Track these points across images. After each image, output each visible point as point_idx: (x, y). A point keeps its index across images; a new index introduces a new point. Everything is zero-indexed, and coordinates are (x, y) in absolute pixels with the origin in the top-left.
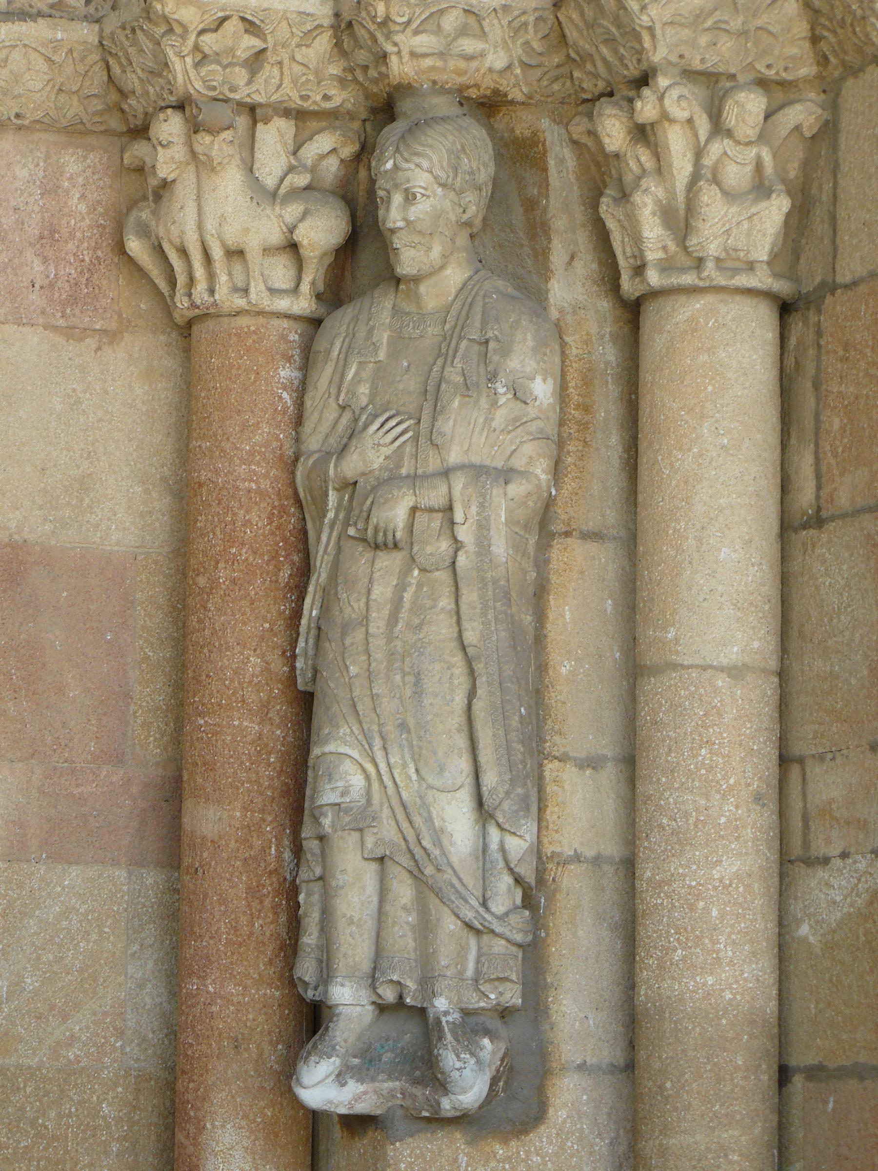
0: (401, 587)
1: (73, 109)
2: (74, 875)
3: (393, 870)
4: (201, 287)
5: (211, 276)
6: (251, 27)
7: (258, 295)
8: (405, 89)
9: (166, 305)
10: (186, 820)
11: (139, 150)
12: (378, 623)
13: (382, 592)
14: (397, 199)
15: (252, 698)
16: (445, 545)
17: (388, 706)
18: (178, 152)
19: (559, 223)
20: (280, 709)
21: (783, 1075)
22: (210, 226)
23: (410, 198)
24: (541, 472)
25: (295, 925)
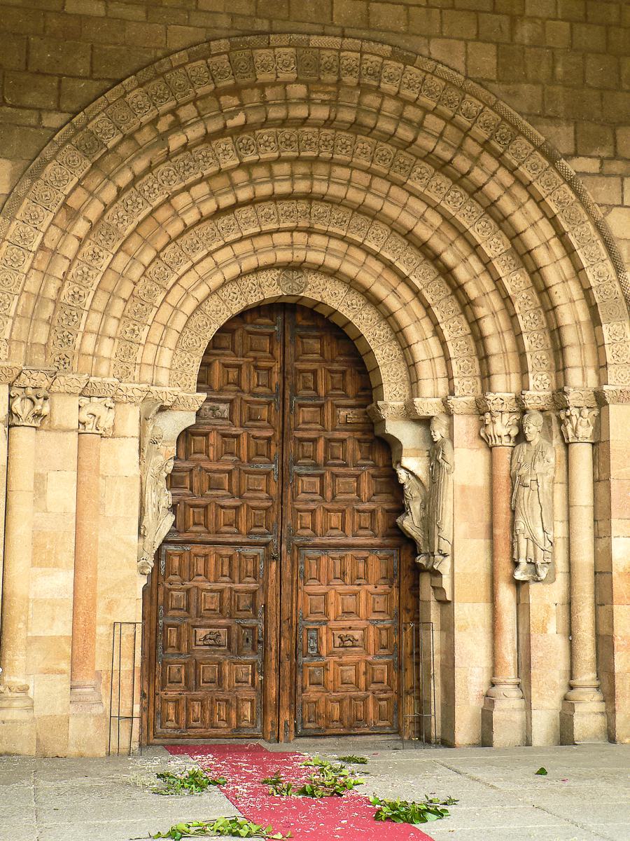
0: (529, 493)
1: (471, 411)
2: (475, 541)
3: (529, 540)
4: (494, 441)
5: (496, 440)
6: (501, 399)
7: (504, 443)
8: (528, 409)
9: (487, 444)
10: (494, 532)
11: (482, 417)
12: (526, 499)
13: (526, 494)
14: (527, 428)
15: (505, 511)
16: (537, 487)
17: (527, 513)
18: (490, 420)
19: (554, 431)
20: (509, 513)
21: (595, 573)
22: (495, 432)
23: (529, 428)
24: (552, 474)
25: (513, 549)
